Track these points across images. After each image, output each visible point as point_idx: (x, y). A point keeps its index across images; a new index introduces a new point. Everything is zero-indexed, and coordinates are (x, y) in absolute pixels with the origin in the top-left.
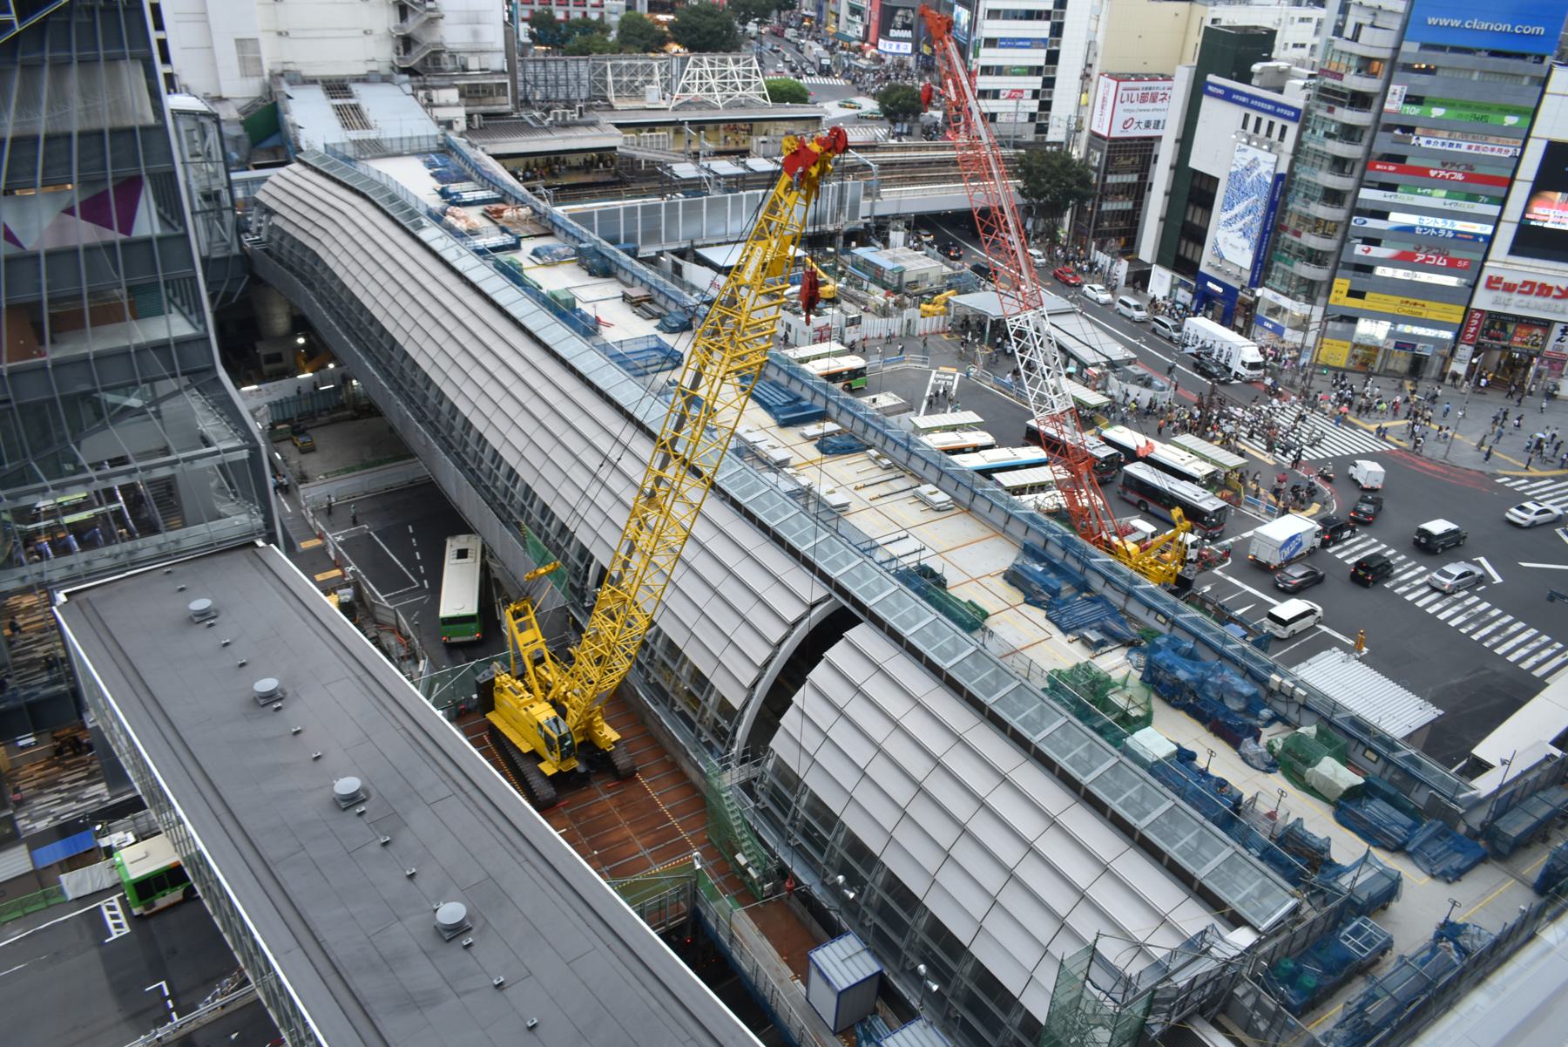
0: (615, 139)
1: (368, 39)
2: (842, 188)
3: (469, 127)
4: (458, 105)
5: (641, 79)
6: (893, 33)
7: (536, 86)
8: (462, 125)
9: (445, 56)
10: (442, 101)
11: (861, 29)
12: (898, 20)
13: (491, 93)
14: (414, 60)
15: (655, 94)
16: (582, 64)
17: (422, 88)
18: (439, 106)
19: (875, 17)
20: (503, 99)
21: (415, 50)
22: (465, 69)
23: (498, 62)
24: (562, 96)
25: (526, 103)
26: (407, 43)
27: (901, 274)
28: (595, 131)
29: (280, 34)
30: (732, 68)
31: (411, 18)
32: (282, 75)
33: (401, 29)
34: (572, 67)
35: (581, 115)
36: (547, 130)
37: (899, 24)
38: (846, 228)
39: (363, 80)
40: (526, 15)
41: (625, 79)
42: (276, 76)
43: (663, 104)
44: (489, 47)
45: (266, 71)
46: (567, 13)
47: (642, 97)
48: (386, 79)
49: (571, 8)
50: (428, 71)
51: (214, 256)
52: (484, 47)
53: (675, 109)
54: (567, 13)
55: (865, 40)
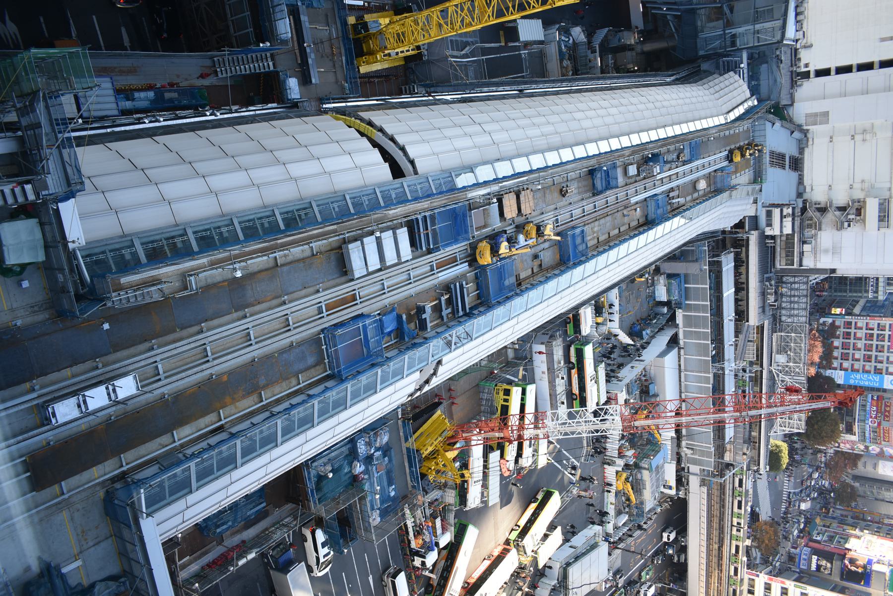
0: (754, 318)
1: (826, 188)
2: (708, 455)
3: (768, 237)
4: (781, 232)
6: (814, 558)
8: (769, 232)
10: (784, 224)
11: (818, 538)
12: (824, 563)
13: (787, 256)
14: (810, 213)
17: (793, 214)
18: (781, 222)
19: (827, 549)
20: (784, 262)
21: (818, 214)
22: (804, 242)
23: (808, 263)
24: (784, 305)
26: (823, 210)
29: (831, 138)
31: (838, 213)
32: (806, 136)
34: (803, 313)
37: (820, 563)
38: (683, 454)
40: (837, 323)
42: (805, 133)
46: (836, 358)
48: (799, 195)
51: (698, 40)
53: (770, 372)
54: (837, 348)
55: (812, 540)
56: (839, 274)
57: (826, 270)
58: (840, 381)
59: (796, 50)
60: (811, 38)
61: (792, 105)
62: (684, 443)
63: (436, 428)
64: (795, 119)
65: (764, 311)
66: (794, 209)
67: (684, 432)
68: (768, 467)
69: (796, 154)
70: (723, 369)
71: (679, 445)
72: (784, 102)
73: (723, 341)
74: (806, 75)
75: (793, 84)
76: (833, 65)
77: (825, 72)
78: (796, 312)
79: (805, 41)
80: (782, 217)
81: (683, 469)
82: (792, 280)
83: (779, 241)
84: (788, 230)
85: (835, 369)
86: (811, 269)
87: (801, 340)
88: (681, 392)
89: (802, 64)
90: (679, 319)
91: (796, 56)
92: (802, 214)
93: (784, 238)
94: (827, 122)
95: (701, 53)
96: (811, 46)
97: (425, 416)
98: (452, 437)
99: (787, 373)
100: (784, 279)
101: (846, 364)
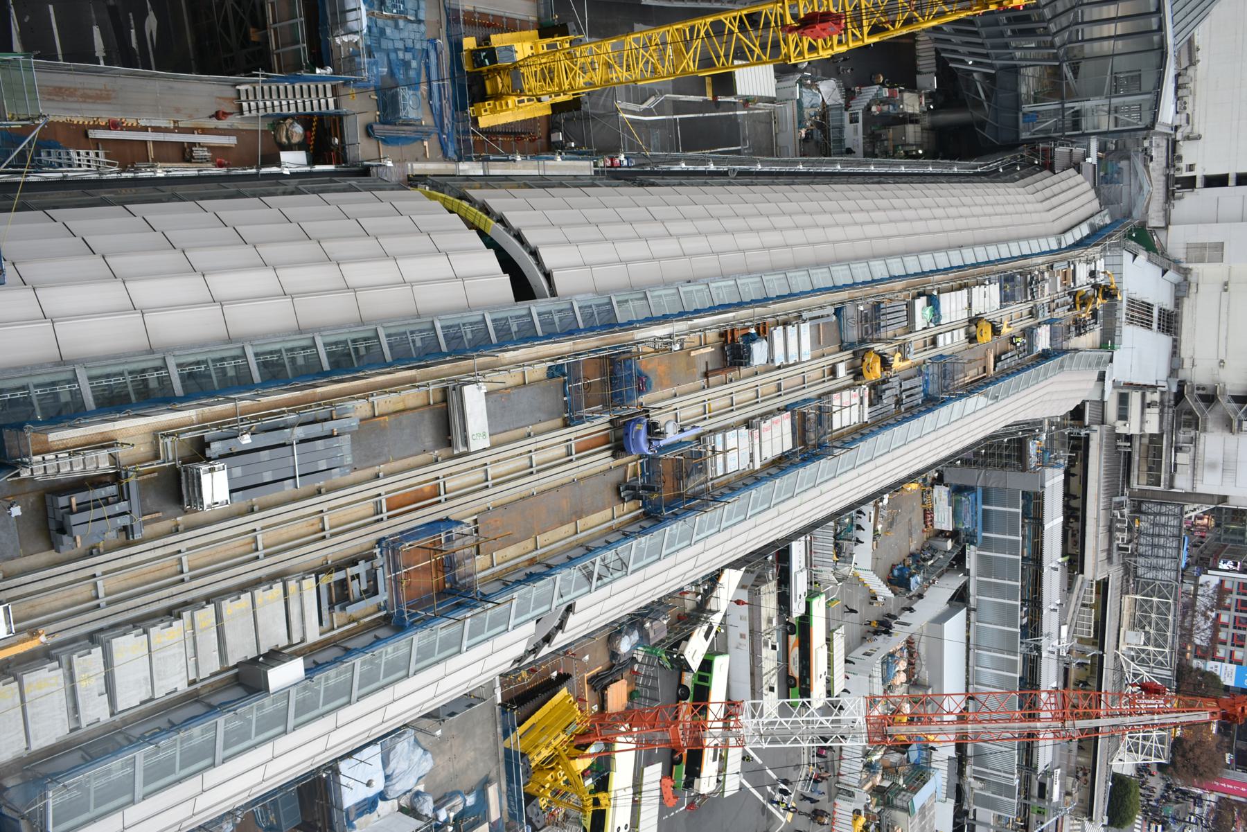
2: (1007, 790)
3: (1119, 436)
4: (1141, 430)
5: (1152, 631)
7: (1154, 525)
8: (1121, 429)
9: (1193, 433)
10: (1147, 417)
13: (1150, 469)
14: (1191, 402)
15: (1135, 641)
16: (1173, 574)
17: (1162, 402)
18: (1143, 413)
20: (1144, 479)
21: (1202, 405)
22: (1178, 449)
23: (1182, 483)
24: (1142, 549)
25: (1137, 510)
26: (1209, 398)
27: (906, 810)
28: (1103, 556)
29: (1226, 284)
30: (1155, 734)
31: (1234, 405)
32: (1186, 279)
33: (1223, 394)
34: (1170, 564)
35: (1120, 549)
36: (1108, 509)
38: (966, 788)
39: (1175, 340)
40: (1227, 585)
41: (1153, 616)
42: (1186, 272)
43: (1123, 647)
44: (1199, 477)
45: (1190, 266)
46: (1224, 643)
47: (1133, 627)
48: (1173, 372)
49: (1233, 613)
50: (1178, 414)
52: (1199, 472)
53: (1116, 657)
56: (1232, 504)
57: (1212, 496)
58: (1229, 681)
59: (1175, 142)
60: (1198, 129)
61: (1166, 228)
62: (968, 770)
63: (557, 719)
64: (1169, 251)
65: (1110, 558)
66: (1163, 393)
67: (970, 750)
68: (1106, 818)
69: (1169, 306)
70: (1038, 649)
71: (961, 773)
72: (1155, 220)
73: (1041, 603)
74: (1190, 183)
75: (1170, 196)
76: (1232, 170)
77: (1218, 181)
78: (1161, 562)
79: (1188, 129)
80: (1145, 405)
81: (967, 813)
82: (1156, 509)
83: (1137, 444)
85: (1222, 660)
86: (1187, 493)
87: (1168, 609)
88: (967, 684)
89: (1183, 165)
90: (971, 563)
91: (1174, 151)
92: (1176, 405)
93: (1146, 441)
95: (1025, 135)
96: (1199, 137)
97: (542, 697)
98: (584, 734)
99: (1143, 662)
100: (1144, 507)
101: (1238, 654)
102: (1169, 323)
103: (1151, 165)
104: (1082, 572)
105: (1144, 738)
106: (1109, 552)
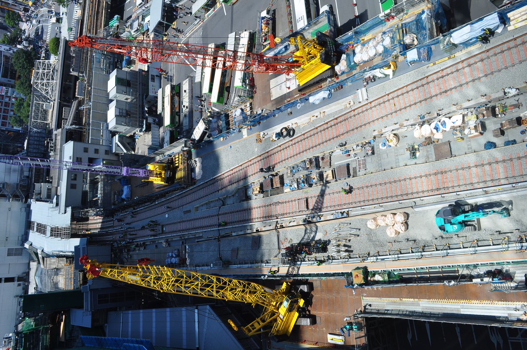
22: (28, 177)
24: (43, 140)
26: (16, 197)
30: (41, 71)
31: (6, 193)
48: (29, 206)
49: (8, 115)
76: (3, 284)
77: (8, 280)
80: (40, 194)
84: (37, 185)
87: (34, 117)
92: (28, 194)
93: (41, 180)
94: (9, 249)
96: (17, 296)
99: (45, 97)
100: (42, 155)
101: (7, 100)
102: (29, 225)
103: (35, 286)
104: (67, 132)
105: (44, 69)
106: (56, 139)
